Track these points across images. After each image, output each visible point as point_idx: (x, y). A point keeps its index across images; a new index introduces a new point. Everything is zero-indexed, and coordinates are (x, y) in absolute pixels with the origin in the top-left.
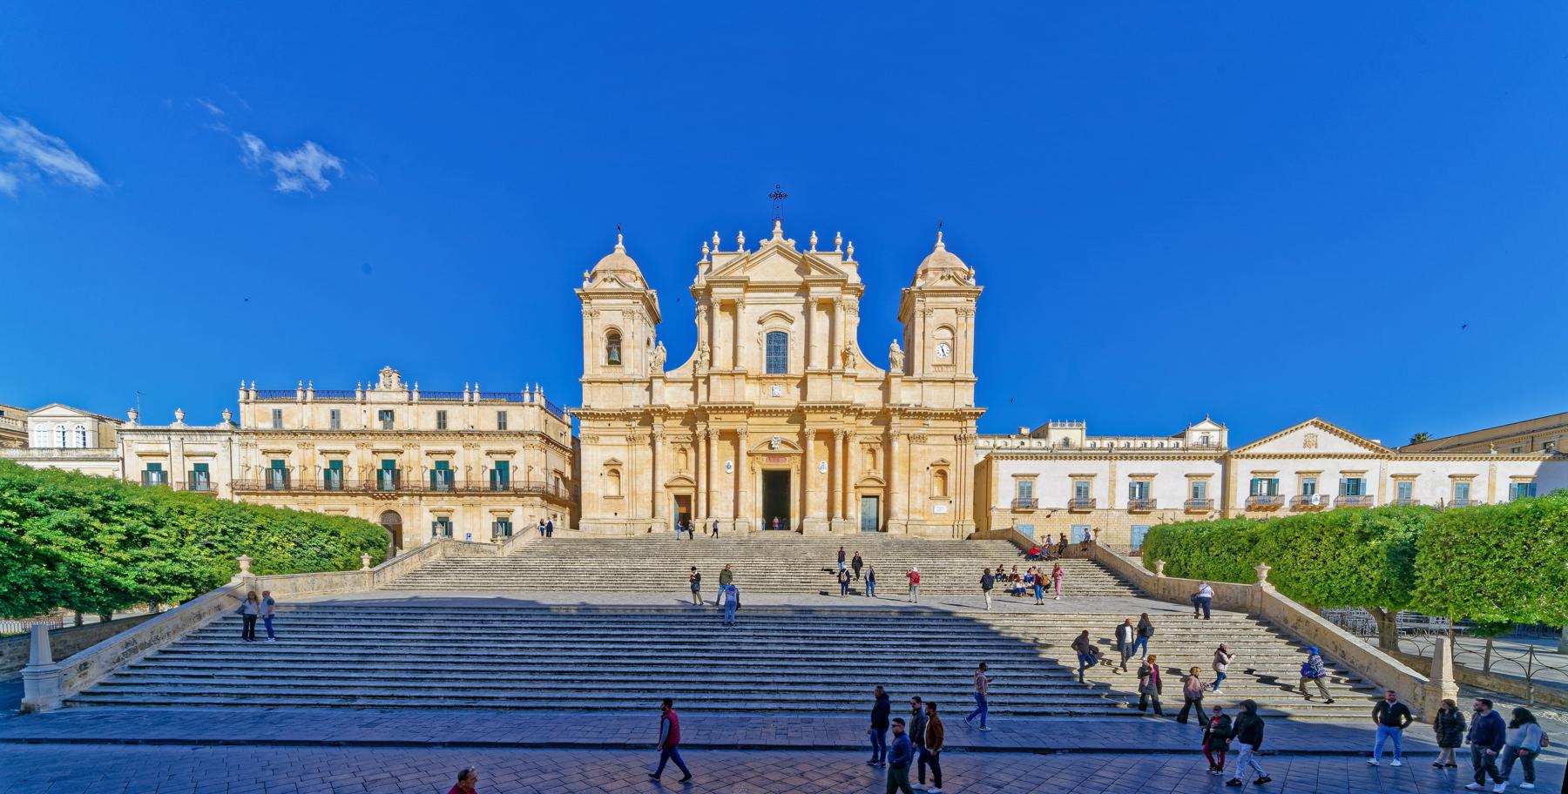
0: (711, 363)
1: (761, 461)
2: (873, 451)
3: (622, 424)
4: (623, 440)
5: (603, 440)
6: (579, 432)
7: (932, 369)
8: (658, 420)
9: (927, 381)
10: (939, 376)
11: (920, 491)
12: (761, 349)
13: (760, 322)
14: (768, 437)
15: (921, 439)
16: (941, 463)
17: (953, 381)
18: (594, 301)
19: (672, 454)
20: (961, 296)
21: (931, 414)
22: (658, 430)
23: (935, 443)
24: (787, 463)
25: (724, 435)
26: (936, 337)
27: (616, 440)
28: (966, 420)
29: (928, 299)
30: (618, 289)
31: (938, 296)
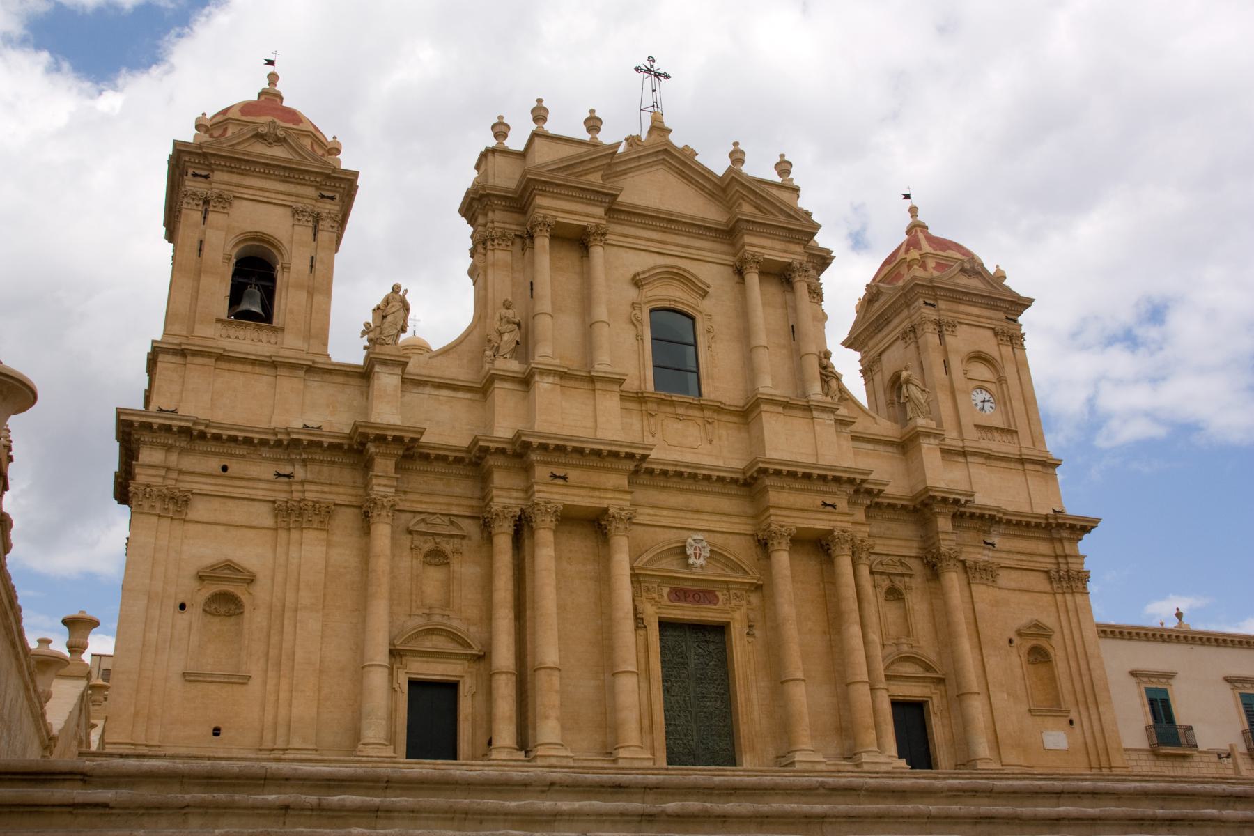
0: (523, 348)
1: (655, 596)
2: (894, 594)
3: (264, 470)
4: (263, 515)
5: (200, 510)
6: (133, 479)
7: (975, 434)
8: (384, 466)
9: (974, 454)
10: (998, 445)
11: (1009, 694)
12: (639, 338)
13: (637, 282)
14: (672, 538)
15: (988, 572)
16: (1033, 631)
17: (1022, 461)
18: (218, 176)
19: (407, 563)
20: (996, 308)
21: (1001, 519)
22: (381, 488)
23: (1013, 585)
24: (720, 605)
25: (569, 519)
26: (969, 375)
27: (239, 513)
28: (1061, 540)
29: (942, 304)
30: (290, 161)
31: (959, 301)
